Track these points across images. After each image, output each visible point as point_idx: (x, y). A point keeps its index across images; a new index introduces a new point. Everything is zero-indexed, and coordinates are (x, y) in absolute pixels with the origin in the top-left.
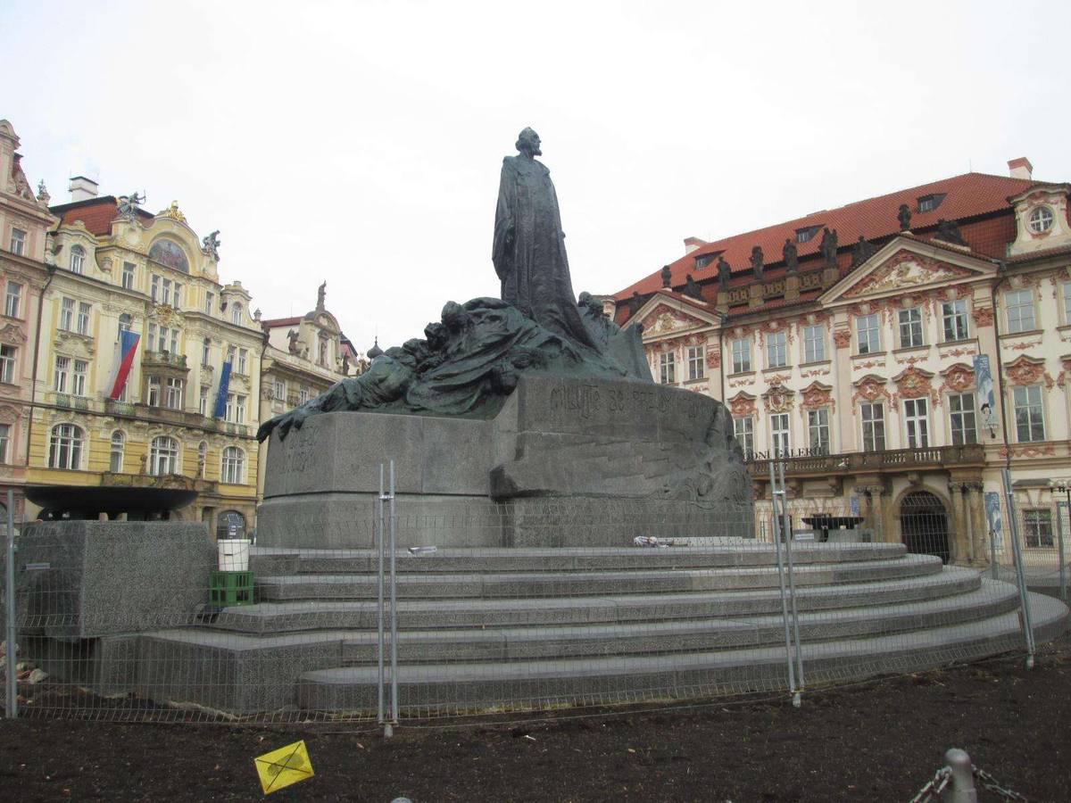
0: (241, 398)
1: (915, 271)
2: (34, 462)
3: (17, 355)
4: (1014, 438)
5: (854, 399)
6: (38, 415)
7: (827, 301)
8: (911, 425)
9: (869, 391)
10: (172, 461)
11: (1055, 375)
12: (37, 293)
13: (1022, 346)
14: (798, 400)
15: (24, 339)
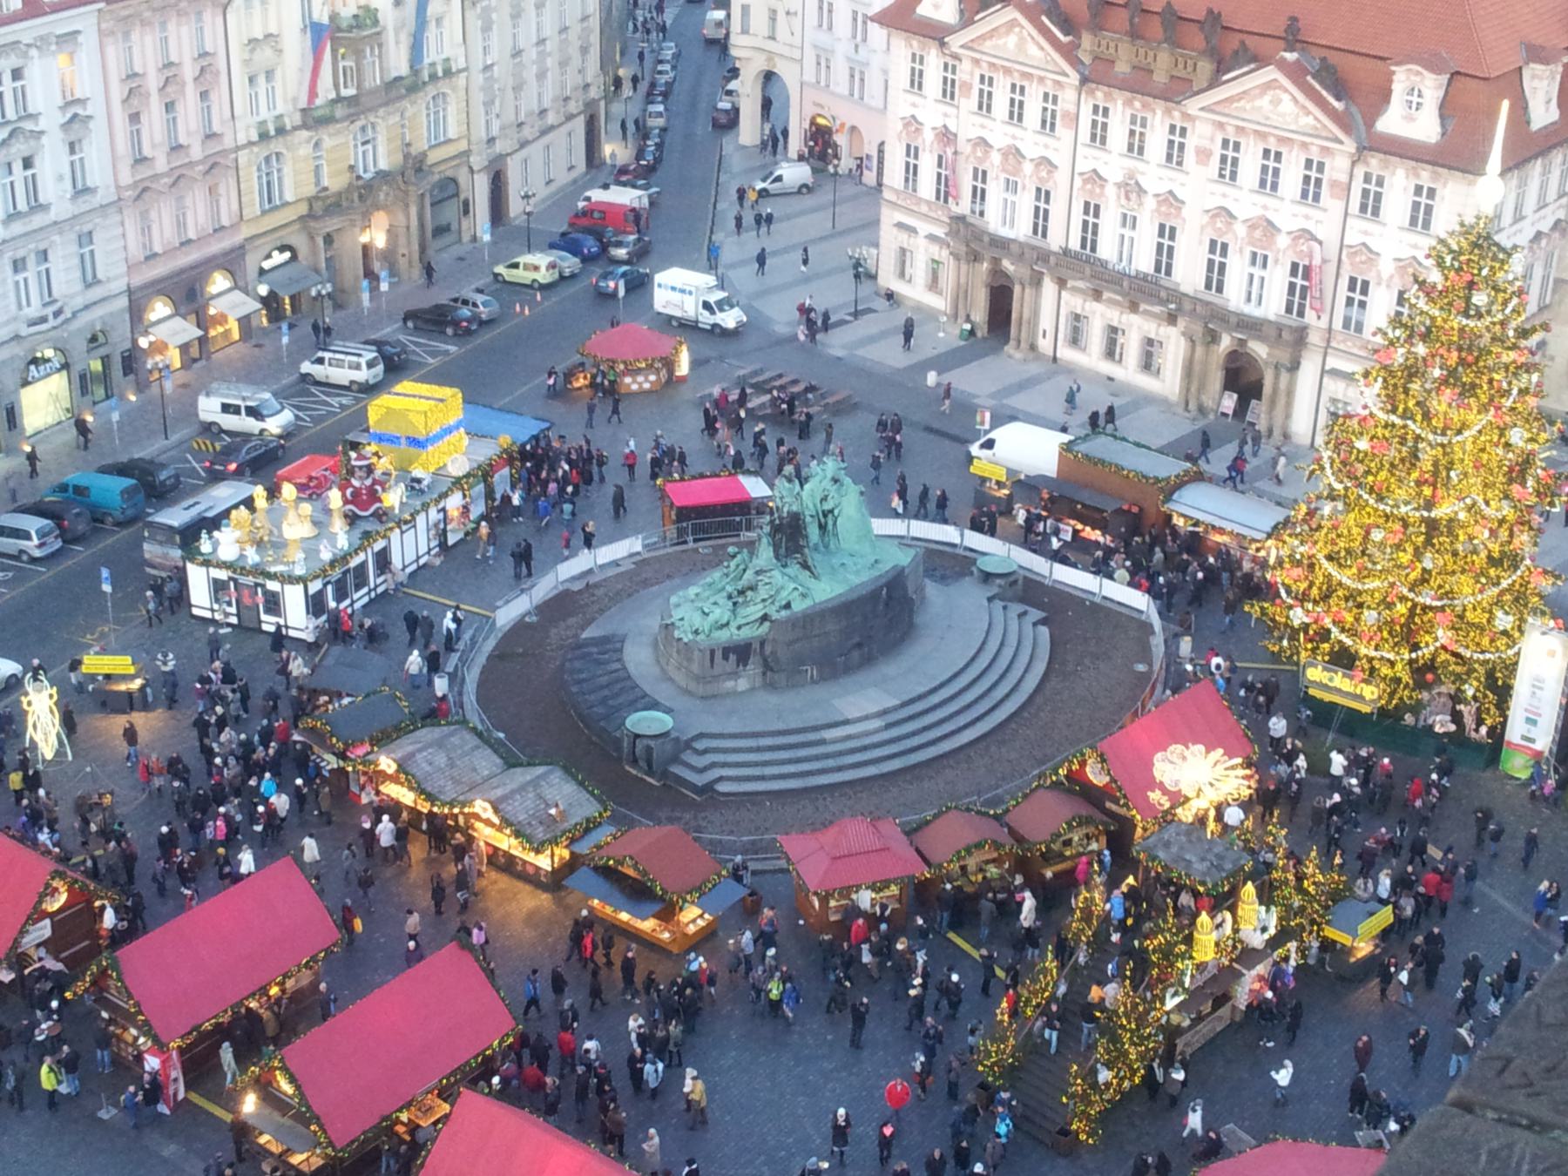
0: (439, 21)
1: (1287, 105)
2: (247, 213)
3: (213, 96)
4: (1338, 324)
5: (1203, 228)
6: (243, 157)
7: (1193, 105)
8: (1251, 276)
9: (1219, 225)
10: (374, 148)
11: (1385, 276)
12: (219, 11)
13: (1366, 233)
14: (1150, 203)
15: (218, 73)
